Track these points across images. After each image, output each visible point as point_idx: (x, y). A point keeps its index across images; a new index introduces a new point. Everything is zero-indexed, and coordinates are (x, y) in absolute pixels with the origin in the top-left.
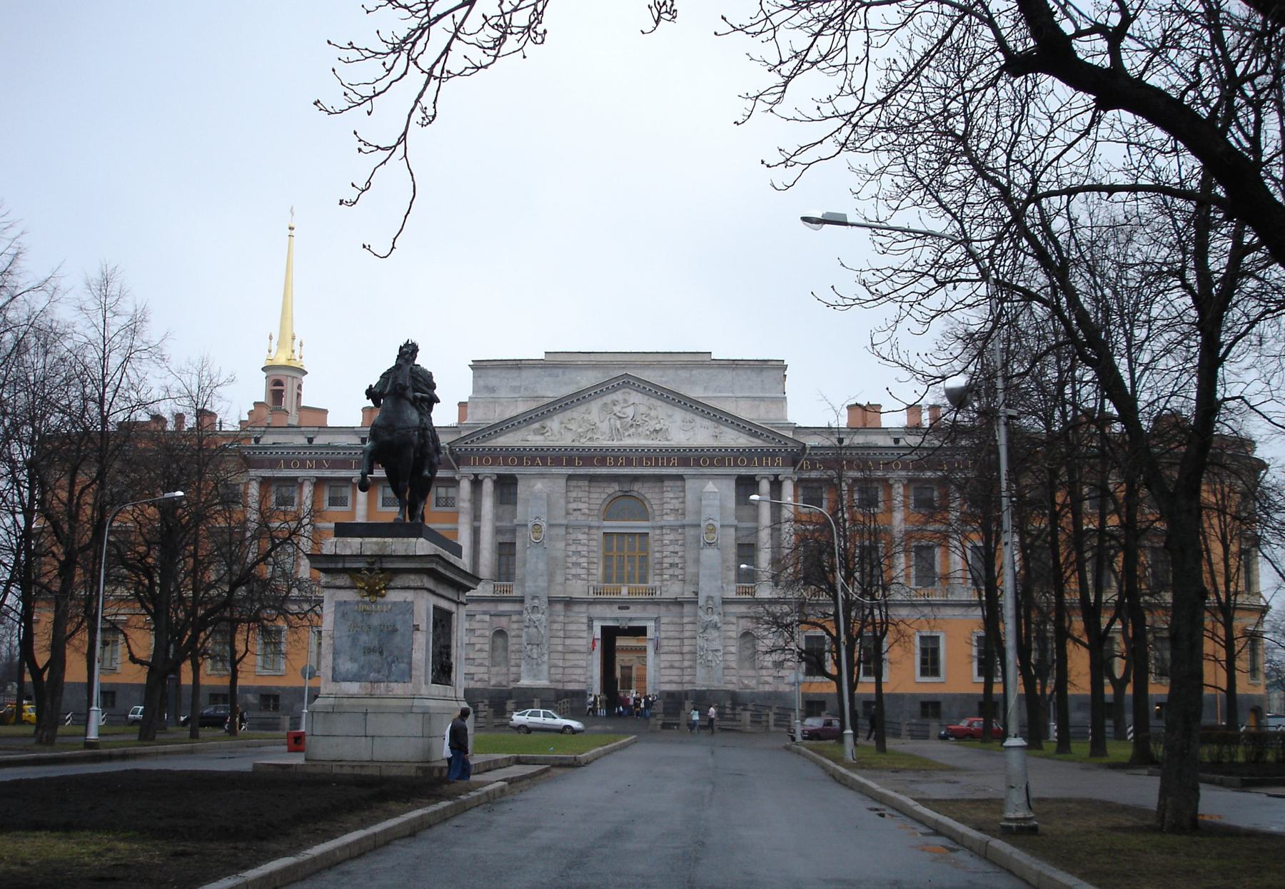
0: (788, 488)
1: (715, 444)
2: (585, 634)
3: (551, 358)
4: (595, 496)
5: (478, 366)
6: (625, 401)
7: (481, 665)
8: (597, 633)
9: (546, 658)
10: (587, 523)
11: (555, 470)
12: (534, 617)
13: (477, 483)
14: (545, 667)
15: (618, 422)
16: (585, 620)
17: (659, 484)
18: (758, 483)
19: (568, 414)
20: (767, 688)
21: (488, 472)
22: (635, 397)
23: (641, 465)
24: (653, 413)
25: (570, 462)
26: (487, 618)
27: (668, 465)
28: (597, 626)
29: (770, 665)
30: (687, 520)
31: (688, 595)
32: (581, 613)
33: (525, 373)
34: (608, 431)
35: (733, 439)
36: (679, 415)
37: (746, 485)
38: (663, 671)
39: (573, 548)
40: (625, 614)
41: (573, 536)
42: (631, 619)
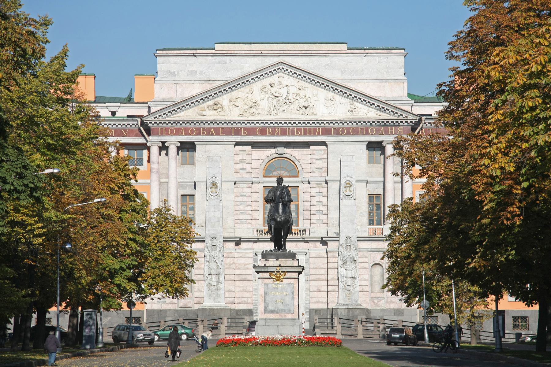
6: (280, 83)
9: (222, 286)
11: (225, 138)
12: (213, 253)
16: (252, 255)
21: (173, 140)
22: (288, 80)
23: (293, 134)
24: (302, 93)
25: (237, 132)
27: (314, 134)
31: (332, 234)
34: (267, 108)
36: (323, 94)
38: (312, 294)
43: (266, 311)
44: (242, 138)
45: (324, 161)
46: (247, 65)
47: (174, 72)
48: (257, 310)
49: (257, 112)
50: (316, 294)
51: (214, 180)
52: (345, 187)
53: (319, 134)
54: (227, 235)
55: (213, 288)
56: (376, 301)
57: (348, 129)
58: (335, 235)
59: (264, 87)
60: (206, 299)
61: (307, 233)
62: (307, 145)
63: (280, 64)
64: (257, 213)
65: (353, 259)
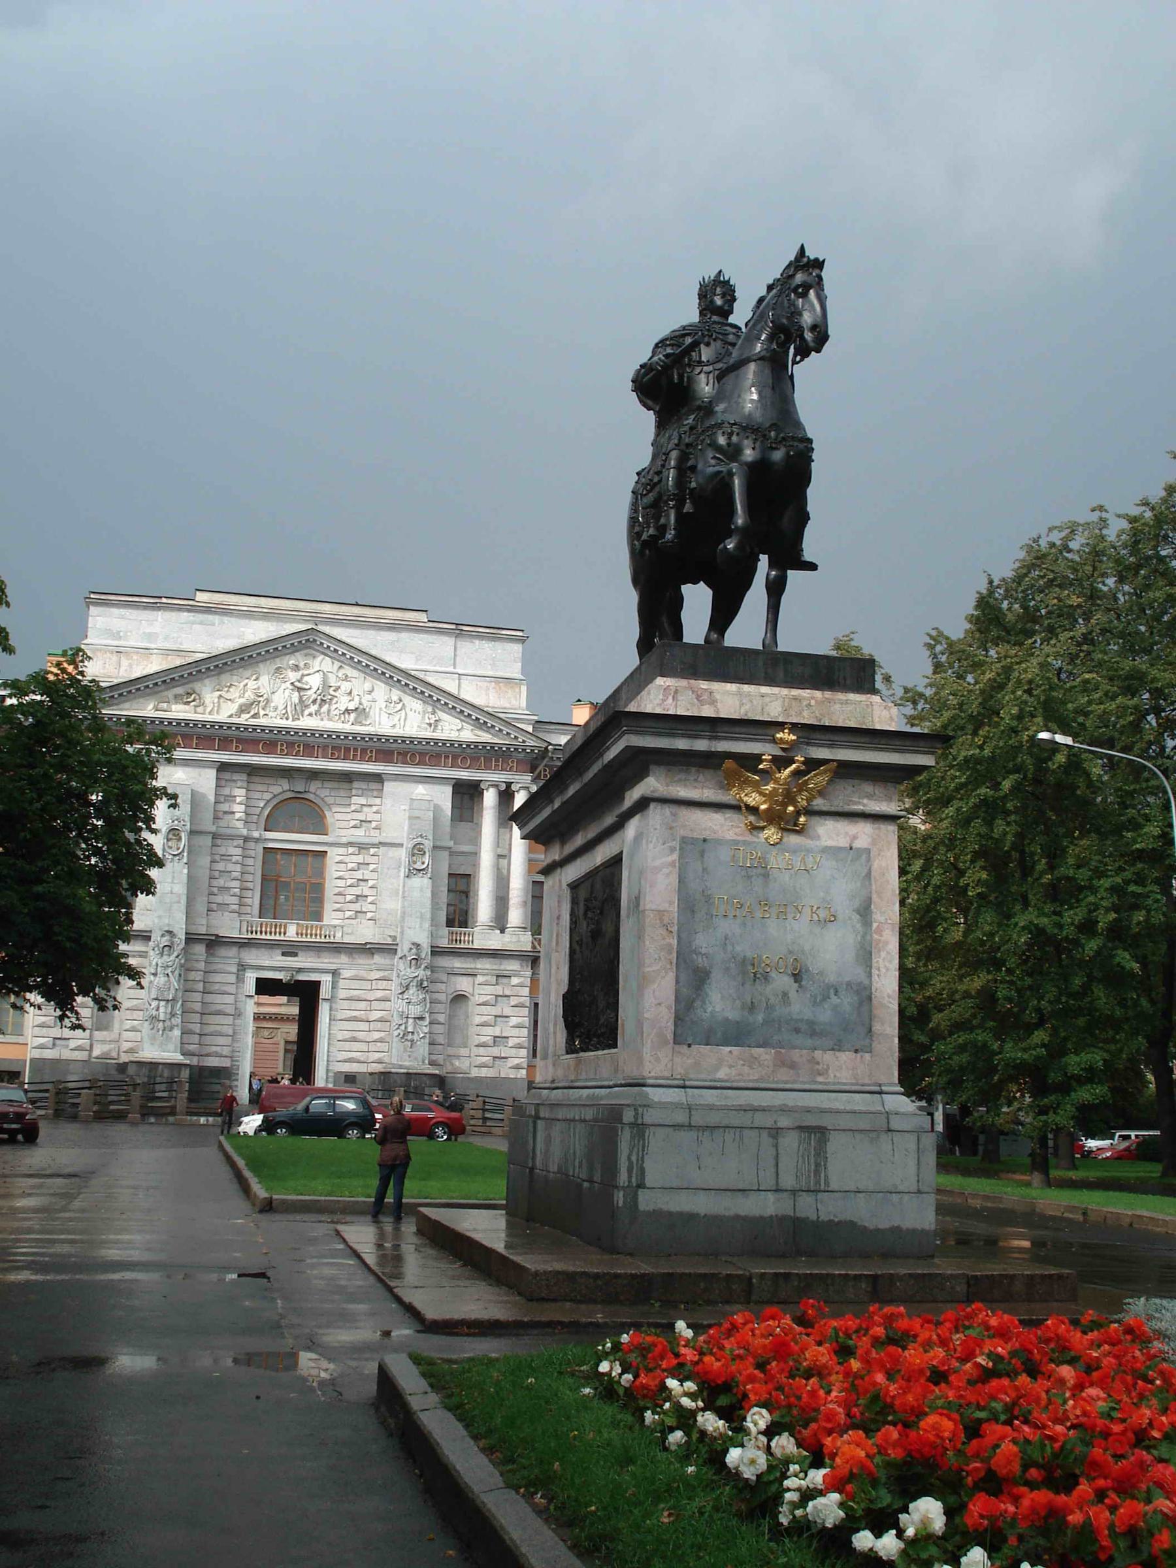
1: (428, 734)
4: (257, 795)
8: (250, 986)
10: (245, 832)
15: (296, 694)
16: (234, 969)
17: (346, 785)
20: (484, 1073)
24: (345, 686)
28: (251, 978)
32: (228, 959)
34: (281, 707)
35: (453, 729)
36: (381, 690)
37: (467, 795)
41: (222, 850)
42: (300, 970)
43: (687, 1028)
45: (375, 809)
46: (251, 631)
47: (119, 632)
50: (347, 1046)
53: (370, 760)
54: (193, 930)
60: (146, 1045)
61: (339, 935)
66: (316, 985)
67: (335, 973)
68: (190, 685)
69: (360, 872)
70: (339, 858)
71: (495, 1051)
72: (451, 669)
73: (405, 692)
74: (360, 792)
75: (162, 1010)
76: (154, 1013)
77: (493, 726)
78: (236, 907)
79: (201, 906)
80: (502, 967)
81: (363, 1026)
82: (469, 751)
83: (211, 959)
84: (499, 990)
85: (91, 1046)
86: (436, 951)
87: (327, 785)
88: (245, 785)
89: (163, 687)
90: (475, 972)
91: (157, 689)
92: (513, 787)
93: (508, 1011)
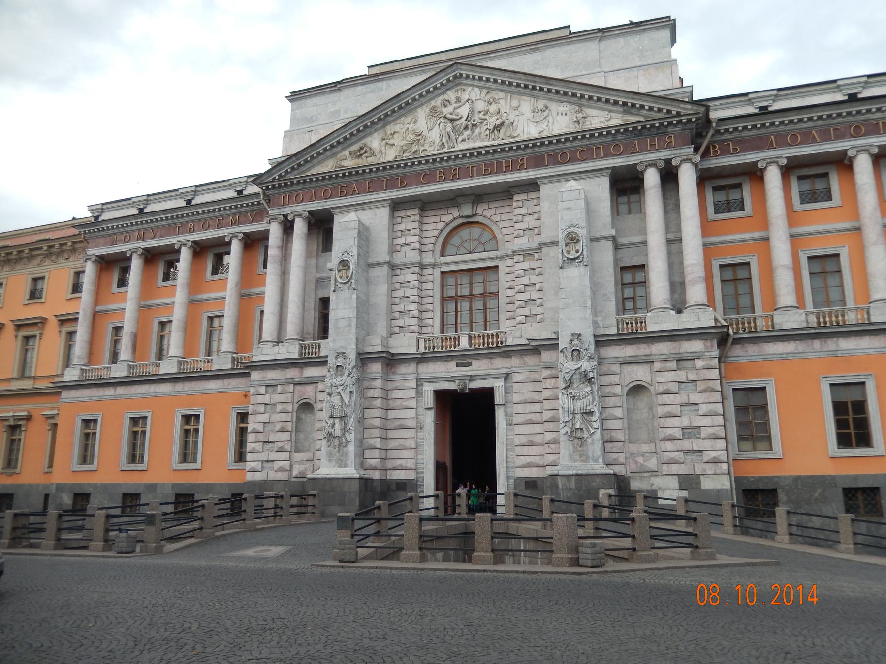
0: (687, 178)
2: (412, 403)
3: (375, 71)
4: (431, 227)
5: (296, 96)
6: (458, 100)
7: (281, 450)
8: (429, 399)
9: (351, 437)
10: (418, 259)
11: (373, 197)
13: (288, 227)
14: (351, 448)
15: (450, 125)
16: (413, 384)
17: (508, 202)
18: (642, 180)
19: (391, 128)
21: (299, 209)
22: (473, 93)
24: (493, 108)
25: (391, 184)
26: (291, 388)
28: (429, 389)
29: (677, 433)
30: (544, 238)
33: (346, 92)
34: (437, 140)
36: (527, 105)
39: (400, 293)
40: (465, 371)
41: (401, 279)
42: (471, 378)
44: (398, 193)
47: (311, 117)
48: (423, 481)
49: (422, 148)
50: (525, 450)
51: (346, 257)
52: (567, 245)
55: (336, 442)
56: (640, 460)
57: (573, 152)
58: (554, 336)
59: (434, 110)
60: (324, 461)
62: (506, 192)
63: (455, 67)
64: (429, 315)
65: (586, 376)
66: (490, 391)
67: (507, 377)
68: (363, 142)
69: (526, 278)
70: (507, 270)
71: (686, 445)
72: (598, 70)
73: (551, 100)
74: (520, 203)
75: (337, 427)
76: (331, 430)
77: (642, 107)
78: (416, 328)
79: (381, 329)
80: (682, 351)
81: (538, 429)
82: (620, 137)
83: (392, 377)
84: (682, 375)
85: (291, 466)
86: (601, 342)
87: (492, 205)
88: (417, 218)
89: (339, 148)
90: (651, 358)
91: (335, 150)
92: (674, 163)
93: (695, 398)
